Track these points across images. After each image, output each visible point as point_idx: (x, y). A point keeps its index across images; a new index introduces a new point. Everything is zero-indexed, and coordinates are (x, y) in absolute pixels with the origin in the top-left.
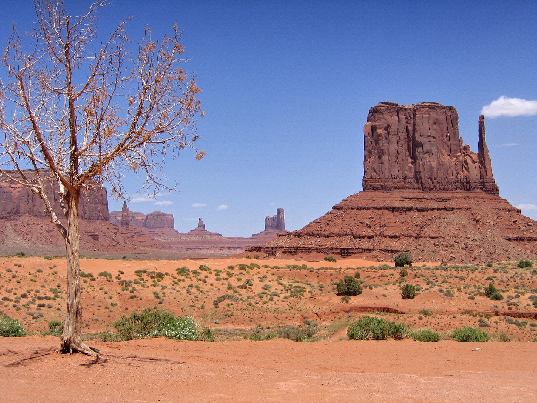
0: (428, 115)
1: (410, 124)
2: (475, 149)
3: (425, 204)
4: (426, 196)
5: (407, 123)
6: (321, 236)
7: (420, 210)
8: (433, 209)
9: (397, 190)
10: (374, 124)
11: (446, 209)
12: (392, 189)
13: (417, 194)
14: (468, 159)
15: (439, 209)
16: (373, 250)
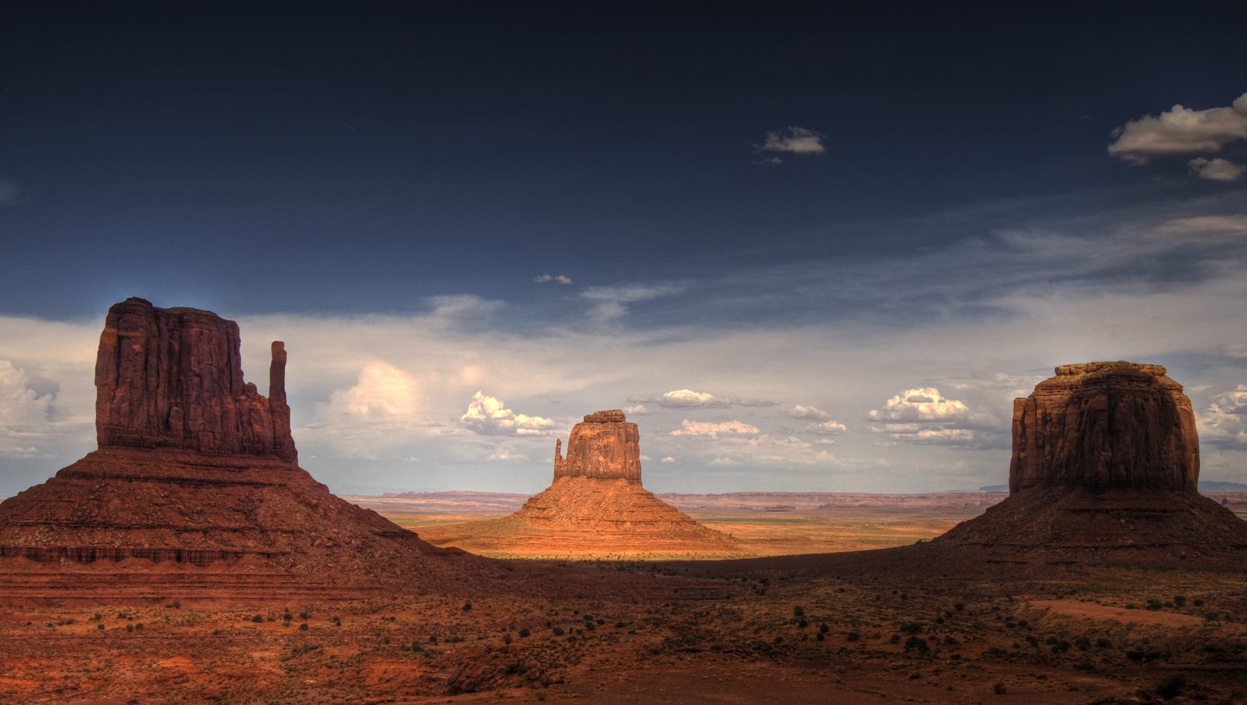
0: (208, 332)
1: (175, 340)
2: (264, 390)
3: (217, 475)
4: (213, 461)
5: (171, 337)
6: (120, 528)
7: (219, 484)
8: (233, 484)
9: (159, 449)
10: (124, 333)
11: (251, 484)
12: (154, 446)
13: (193, 458)
14: (259, 406)
15: (241, 484)
16: (244, 553)
